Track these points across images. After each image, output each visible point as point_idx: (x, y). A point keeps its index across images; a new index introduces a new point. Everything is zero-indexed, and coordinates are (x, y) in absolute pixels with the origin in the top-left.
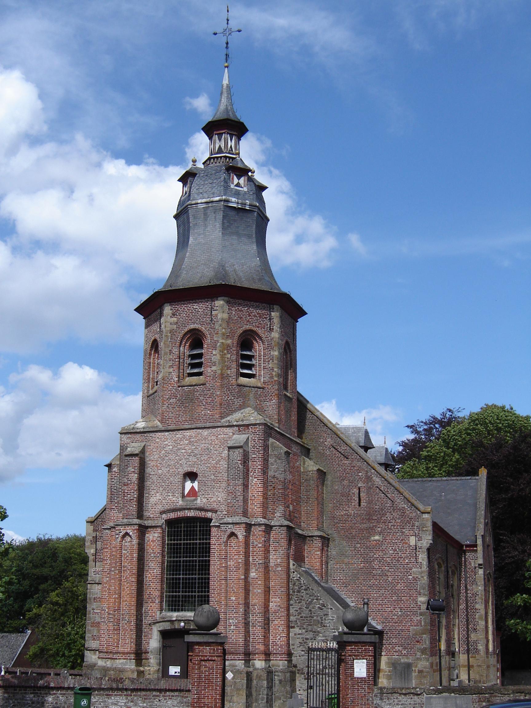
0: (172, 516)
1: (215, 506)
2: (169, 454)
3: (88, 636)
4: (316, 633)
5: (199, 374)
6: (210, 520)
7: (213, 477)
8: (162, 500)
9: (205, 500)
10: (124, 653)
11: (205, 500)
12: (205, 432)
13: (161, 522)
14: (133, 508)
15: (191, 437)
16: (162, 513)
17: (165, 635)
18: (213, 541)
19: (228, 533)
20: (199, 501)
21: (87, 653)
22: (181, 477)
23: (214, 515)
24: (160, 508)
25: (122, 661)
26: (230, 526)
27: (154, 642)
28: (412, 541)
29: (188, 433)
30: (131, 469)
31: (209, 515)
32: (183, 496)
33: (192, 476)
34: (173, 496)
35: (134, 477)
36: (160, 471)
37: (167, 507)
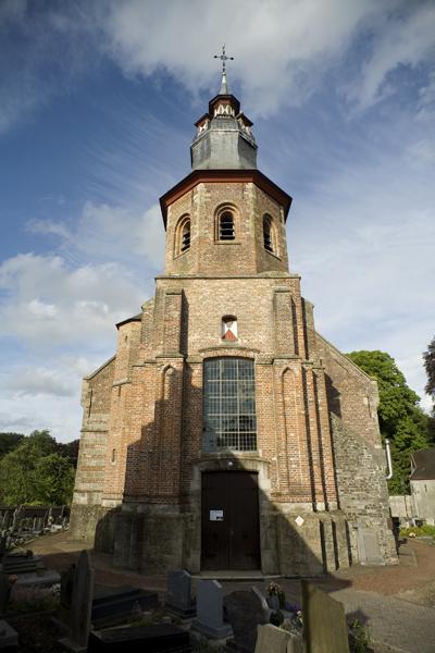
0: (211, 354)
1: (256, 346)
2: (207, 300)
3: (77, 479)
4: (354, 473)
5: (233, 238)
6: (253, 360)
7: (253, 321)
8: (202, 339)
9: (245, 341)
10: (165, 497)
11: (245, 341)
12: (244, 282)
13: (201, 360)
14: (175, 342)
15: (228, 285)
16: (201, 351)
17: (204, 474)
18: (258, 377)
19: (284, 367)
20: (239, 341)
21: (76, 495)
22: (219, 320)
23: (256, 354)
24: (198, 346)
25: (162, 507)
26: (285, 361)
27: (195, 485)
28: (366, 401)
29: (225, 282)
30: (172, 307)
31: (251, 355)
32: (224, 338)
33: (228, 319)
34: (212, 335)
35: (177, 314)
36: (198, 314)
37: (208, 346)
